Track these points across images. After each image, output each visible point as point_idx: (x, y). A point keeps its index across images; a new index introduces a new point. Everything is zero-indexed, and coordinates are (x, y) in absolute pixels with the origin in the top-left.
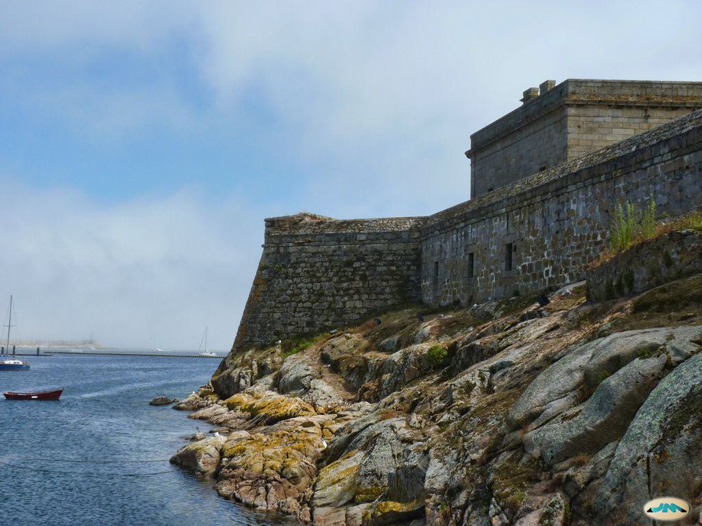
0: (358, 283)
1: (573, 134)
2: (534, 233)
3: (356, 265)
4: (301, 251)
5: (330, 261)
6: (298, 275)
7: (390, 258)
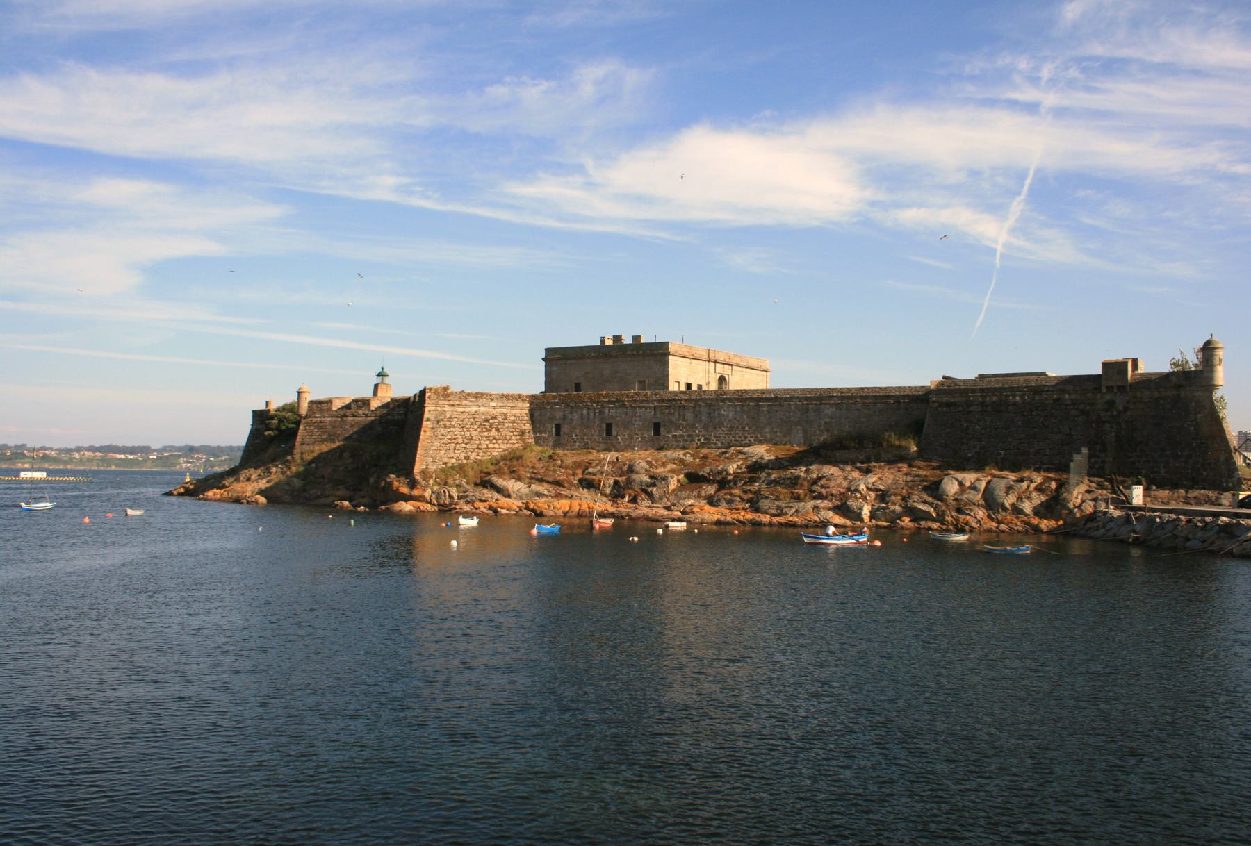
0: (494, 433)
2: (684, 420)
3: (491, 421)
5: (474, 418)
6: (454, 427)
7: (512, 418)
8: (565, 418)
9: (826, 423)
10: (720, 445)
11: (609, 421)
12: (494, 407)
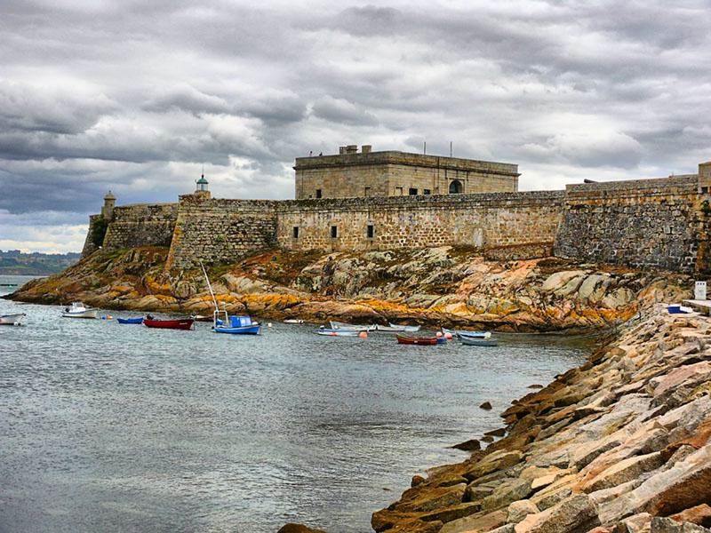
0: (241, 235)
1: (391, 177)
3: (239, 225)
4: (203, 216)
6: (203, 229)
7: (259, 222)
8: (301, 221)
9: (501, 225)
10: (418, 245)
11: (334, 225)
12: (242, 213)
